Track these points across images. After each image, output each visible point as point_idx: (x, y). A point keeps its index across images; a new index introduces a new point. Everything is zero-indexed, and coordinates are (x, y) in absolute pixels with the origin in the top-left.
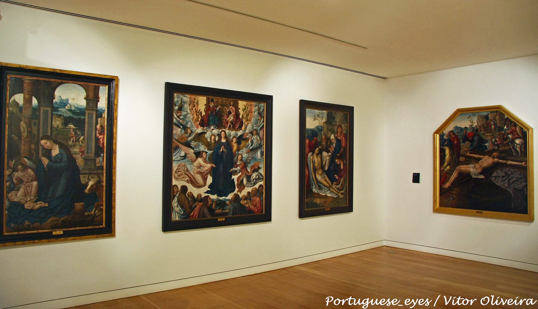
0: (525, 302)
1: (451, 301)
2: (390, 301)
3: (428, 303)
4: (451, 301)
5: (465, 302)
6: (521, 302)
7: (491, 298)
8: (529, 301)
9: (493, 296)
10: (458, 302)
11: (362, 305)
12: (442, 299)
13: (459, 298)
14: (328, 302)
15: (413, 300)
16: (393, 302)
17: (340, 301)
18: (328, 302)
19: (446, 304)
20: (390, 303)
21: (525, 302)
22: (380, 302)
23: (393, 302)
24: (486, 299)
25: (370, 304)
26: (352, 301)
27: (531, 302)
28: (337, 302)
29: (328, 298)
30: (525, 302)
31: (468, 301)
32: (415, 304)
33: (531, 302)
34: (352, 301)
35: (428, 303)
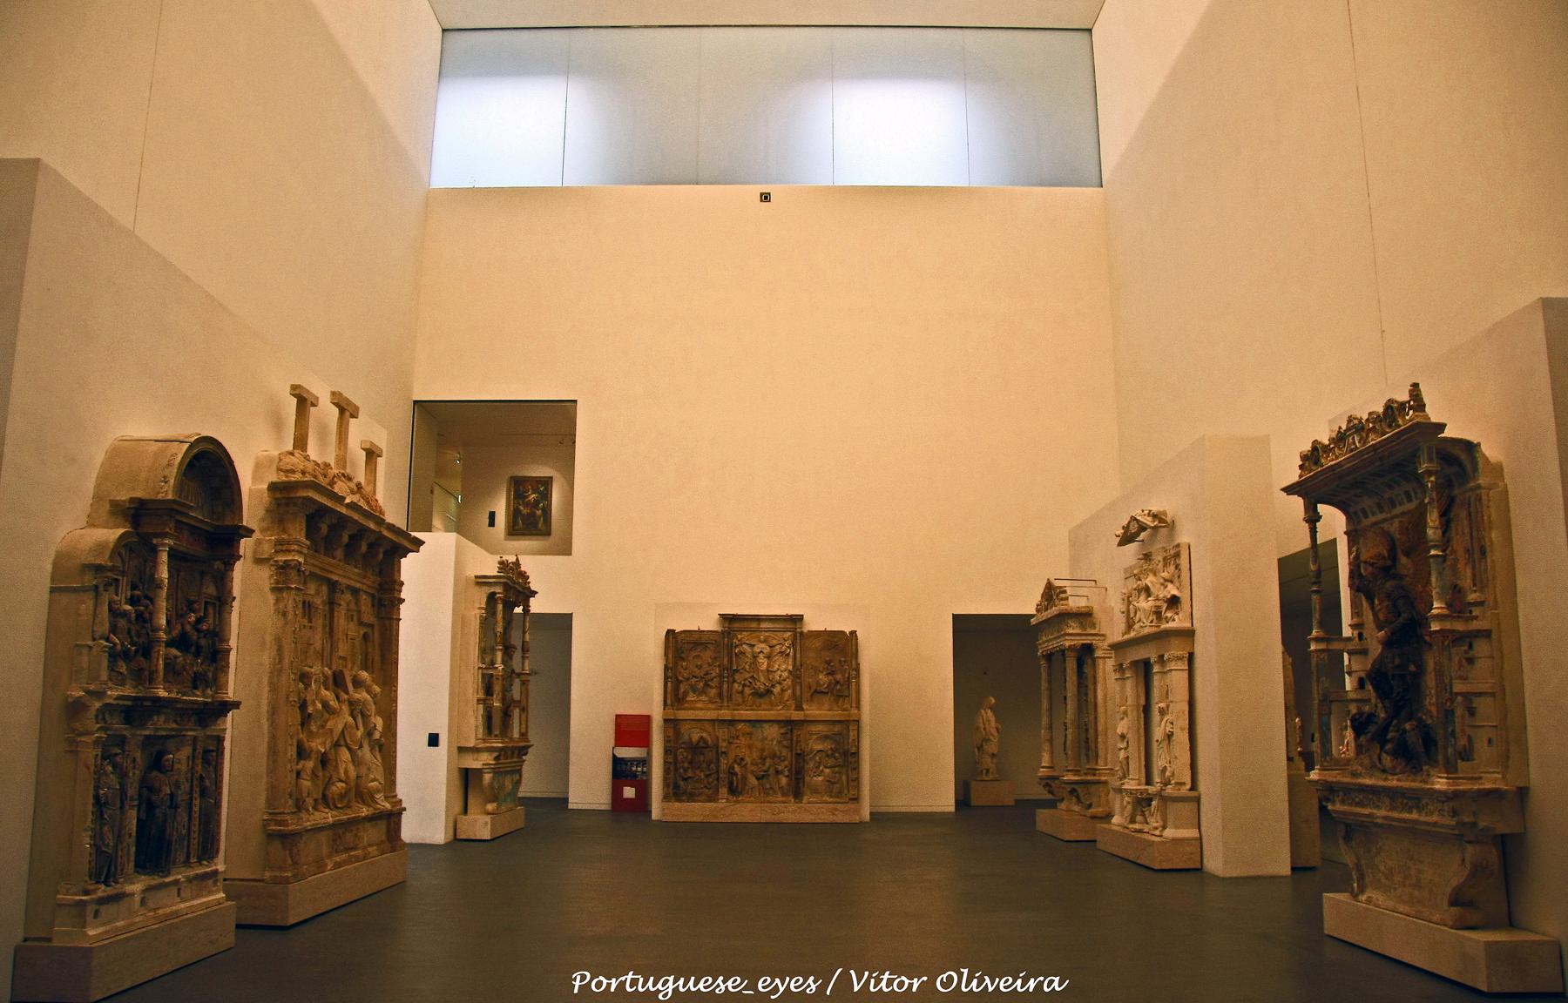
0: (1040, 984)
1: (868, 981)
2: (724, 982)
3: (812, 986)
4: (868, 981)
5: (901, 984)
6: (1032, 984)
7: (960, 976)
8: (1052, 982)
9: (966, 971)
10: (883, 984)
11: (659, 991)
12: (845, 977)
13: (886, 976)
14: (577, 984)
15: (777, 981)
16: (729, 983)
17: (605, 982)
18: (577, 984)
19: (856, 988)
20: (723, 987)
21: (1040, 984)
22: (701, 986)
23: (731, 985)
24: (950, 978)
25: (676, 990)
26: (634, 982)
27: (1056, 984)
28: (599, 984)
29: (577, 976)
30: (1041, 983)
31: (907, 982)
32: (782, 989)
33: (1056, 984)
34: (634, 982)
35: (813, 987)
